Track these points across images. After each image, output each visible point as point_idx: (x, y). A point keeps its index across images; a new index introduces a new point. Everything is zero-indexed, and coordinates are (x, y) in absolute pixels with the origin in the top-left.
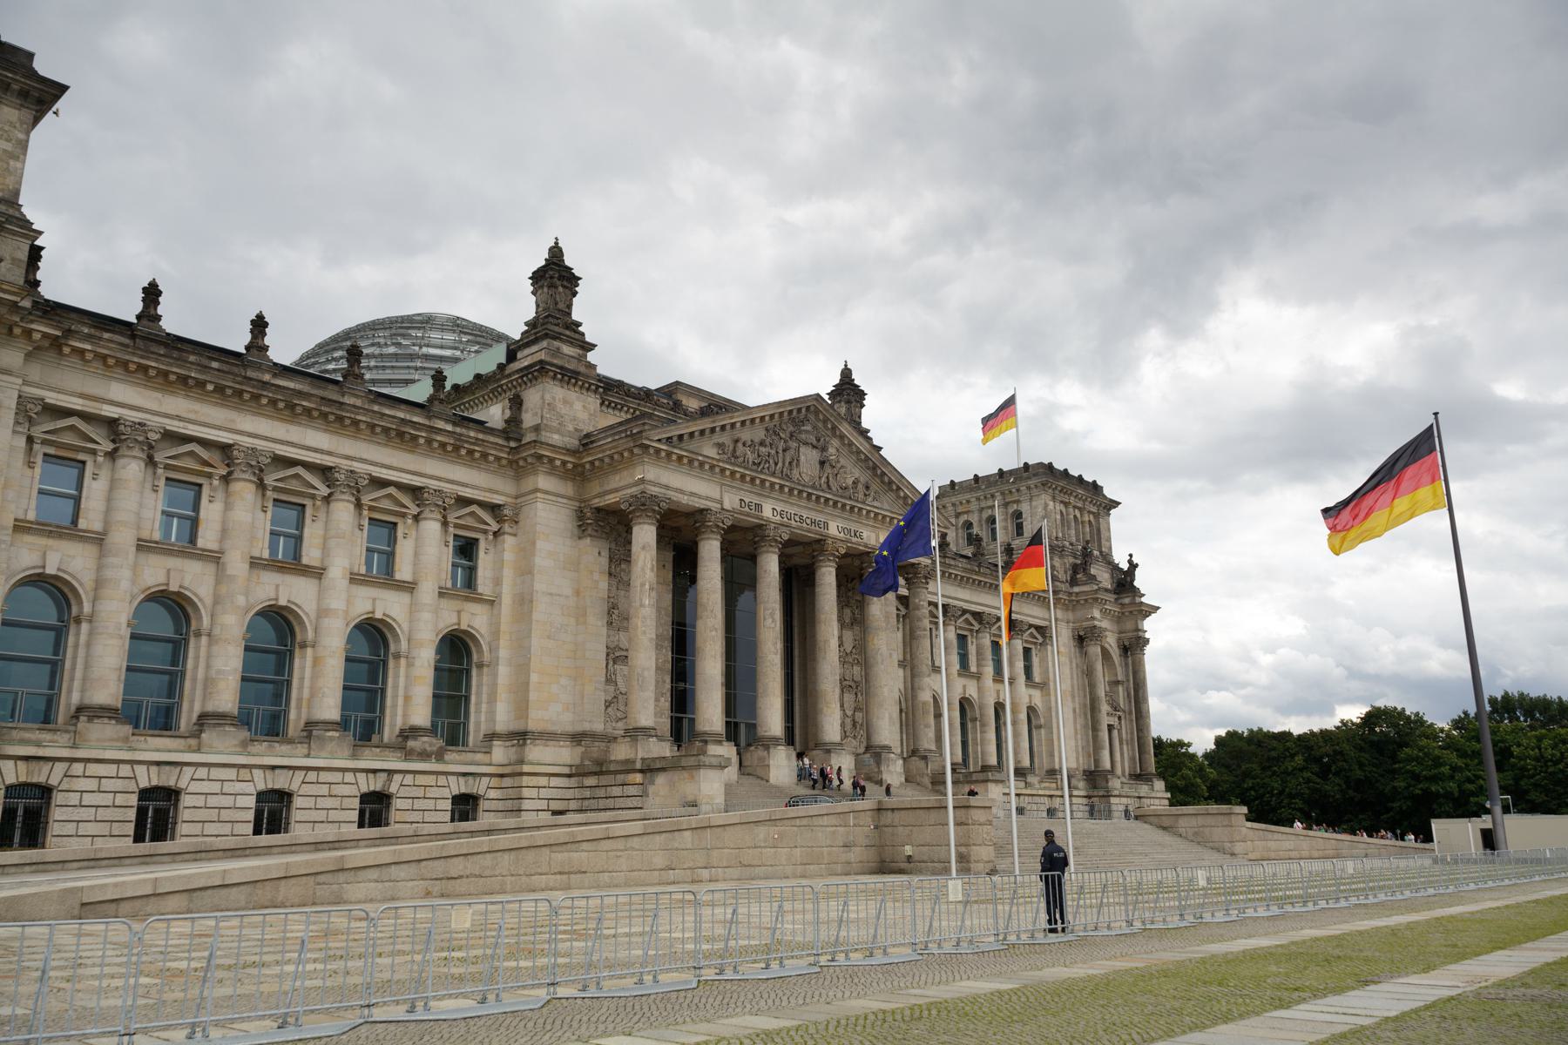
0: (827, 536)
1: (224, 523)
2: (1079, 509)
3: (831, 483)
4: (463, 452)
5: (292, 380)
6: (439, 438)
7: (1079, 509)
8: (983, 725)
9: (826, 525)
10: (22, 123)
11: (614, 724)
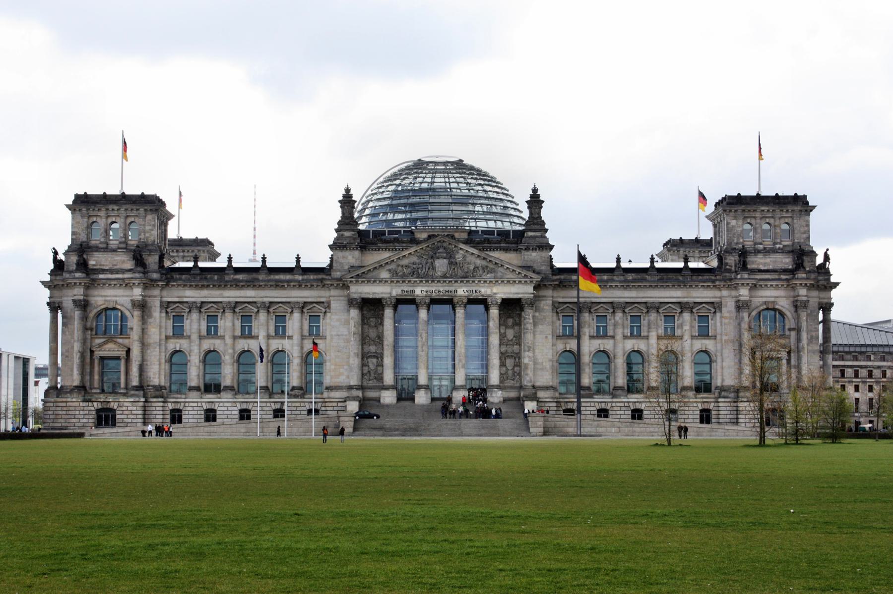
0: (455, 296)
1: (225, 326)
2: (772, 217)
4: (303, 286)
5: (241, 274)
6: (292, 284)
7: (772, 217)
8: (649, 365)
9: (456, 291)
10: (153, 218)
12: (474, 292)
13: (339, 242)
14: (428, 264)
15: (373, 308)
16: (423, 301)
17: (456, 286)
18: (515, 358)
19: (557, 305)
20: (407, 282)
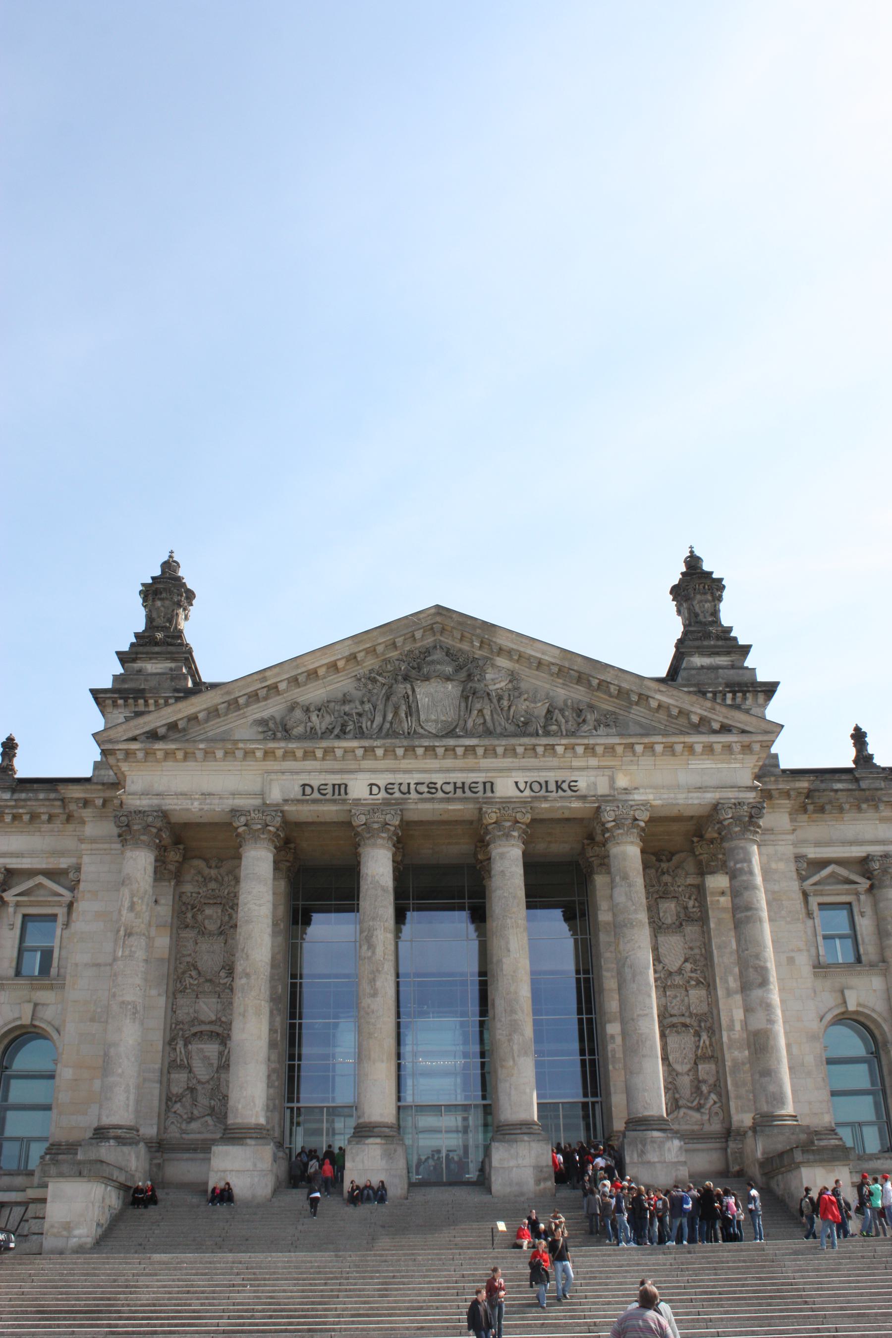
0: (489, 802)
3: (490, 724)
4: (8, 818)
9: (489, 786)
11: (184, 1126)
12: (552, 787)
13: (126, 686)
14: (394, 699)
15: (213, 872)
16: (379, 817)
17: (488, 770)
18: (697, 1034)
19: (805, 865)
20: (319, 753)
